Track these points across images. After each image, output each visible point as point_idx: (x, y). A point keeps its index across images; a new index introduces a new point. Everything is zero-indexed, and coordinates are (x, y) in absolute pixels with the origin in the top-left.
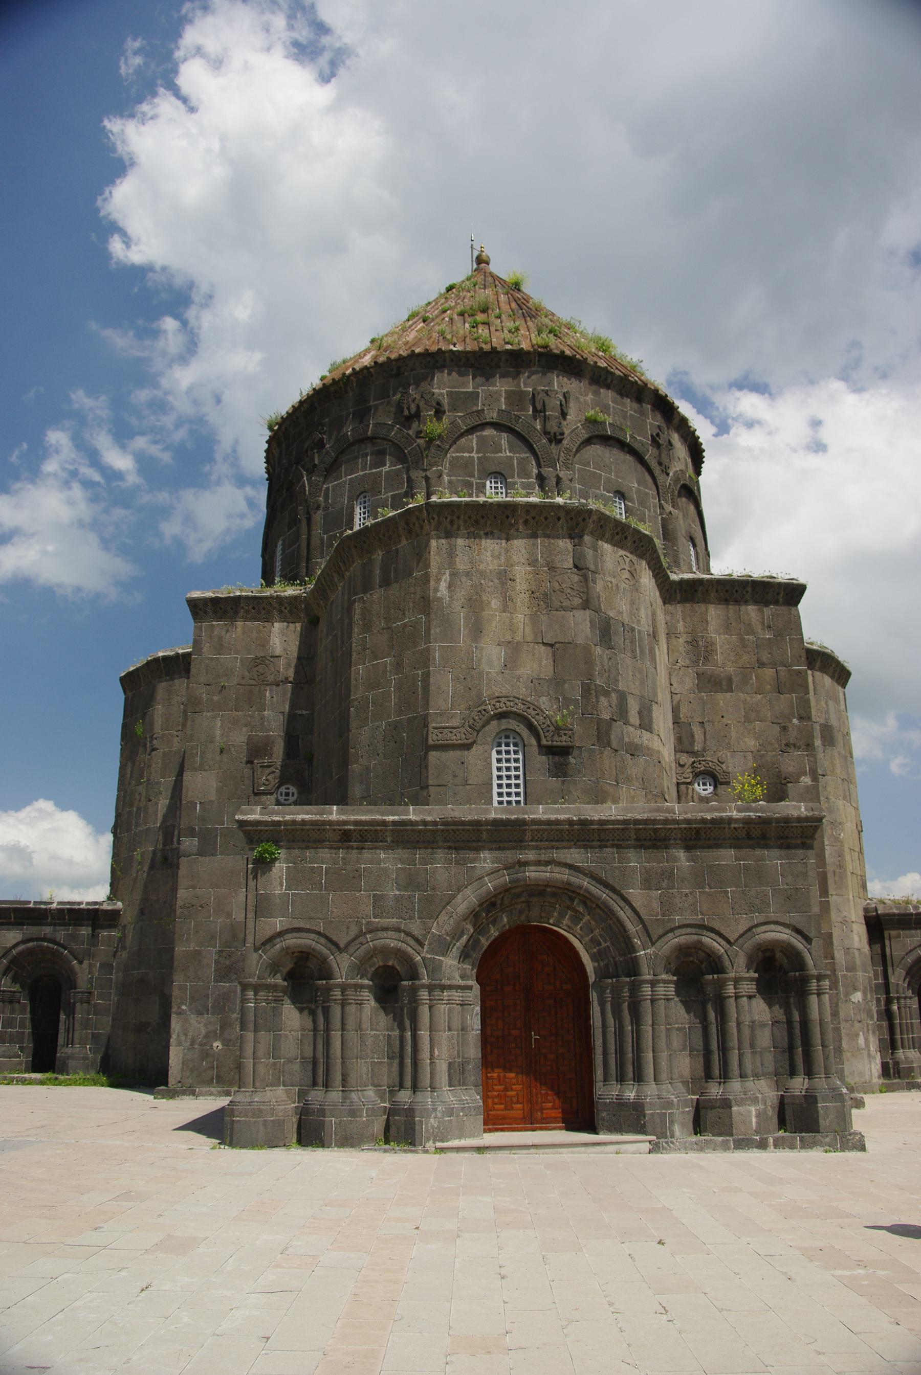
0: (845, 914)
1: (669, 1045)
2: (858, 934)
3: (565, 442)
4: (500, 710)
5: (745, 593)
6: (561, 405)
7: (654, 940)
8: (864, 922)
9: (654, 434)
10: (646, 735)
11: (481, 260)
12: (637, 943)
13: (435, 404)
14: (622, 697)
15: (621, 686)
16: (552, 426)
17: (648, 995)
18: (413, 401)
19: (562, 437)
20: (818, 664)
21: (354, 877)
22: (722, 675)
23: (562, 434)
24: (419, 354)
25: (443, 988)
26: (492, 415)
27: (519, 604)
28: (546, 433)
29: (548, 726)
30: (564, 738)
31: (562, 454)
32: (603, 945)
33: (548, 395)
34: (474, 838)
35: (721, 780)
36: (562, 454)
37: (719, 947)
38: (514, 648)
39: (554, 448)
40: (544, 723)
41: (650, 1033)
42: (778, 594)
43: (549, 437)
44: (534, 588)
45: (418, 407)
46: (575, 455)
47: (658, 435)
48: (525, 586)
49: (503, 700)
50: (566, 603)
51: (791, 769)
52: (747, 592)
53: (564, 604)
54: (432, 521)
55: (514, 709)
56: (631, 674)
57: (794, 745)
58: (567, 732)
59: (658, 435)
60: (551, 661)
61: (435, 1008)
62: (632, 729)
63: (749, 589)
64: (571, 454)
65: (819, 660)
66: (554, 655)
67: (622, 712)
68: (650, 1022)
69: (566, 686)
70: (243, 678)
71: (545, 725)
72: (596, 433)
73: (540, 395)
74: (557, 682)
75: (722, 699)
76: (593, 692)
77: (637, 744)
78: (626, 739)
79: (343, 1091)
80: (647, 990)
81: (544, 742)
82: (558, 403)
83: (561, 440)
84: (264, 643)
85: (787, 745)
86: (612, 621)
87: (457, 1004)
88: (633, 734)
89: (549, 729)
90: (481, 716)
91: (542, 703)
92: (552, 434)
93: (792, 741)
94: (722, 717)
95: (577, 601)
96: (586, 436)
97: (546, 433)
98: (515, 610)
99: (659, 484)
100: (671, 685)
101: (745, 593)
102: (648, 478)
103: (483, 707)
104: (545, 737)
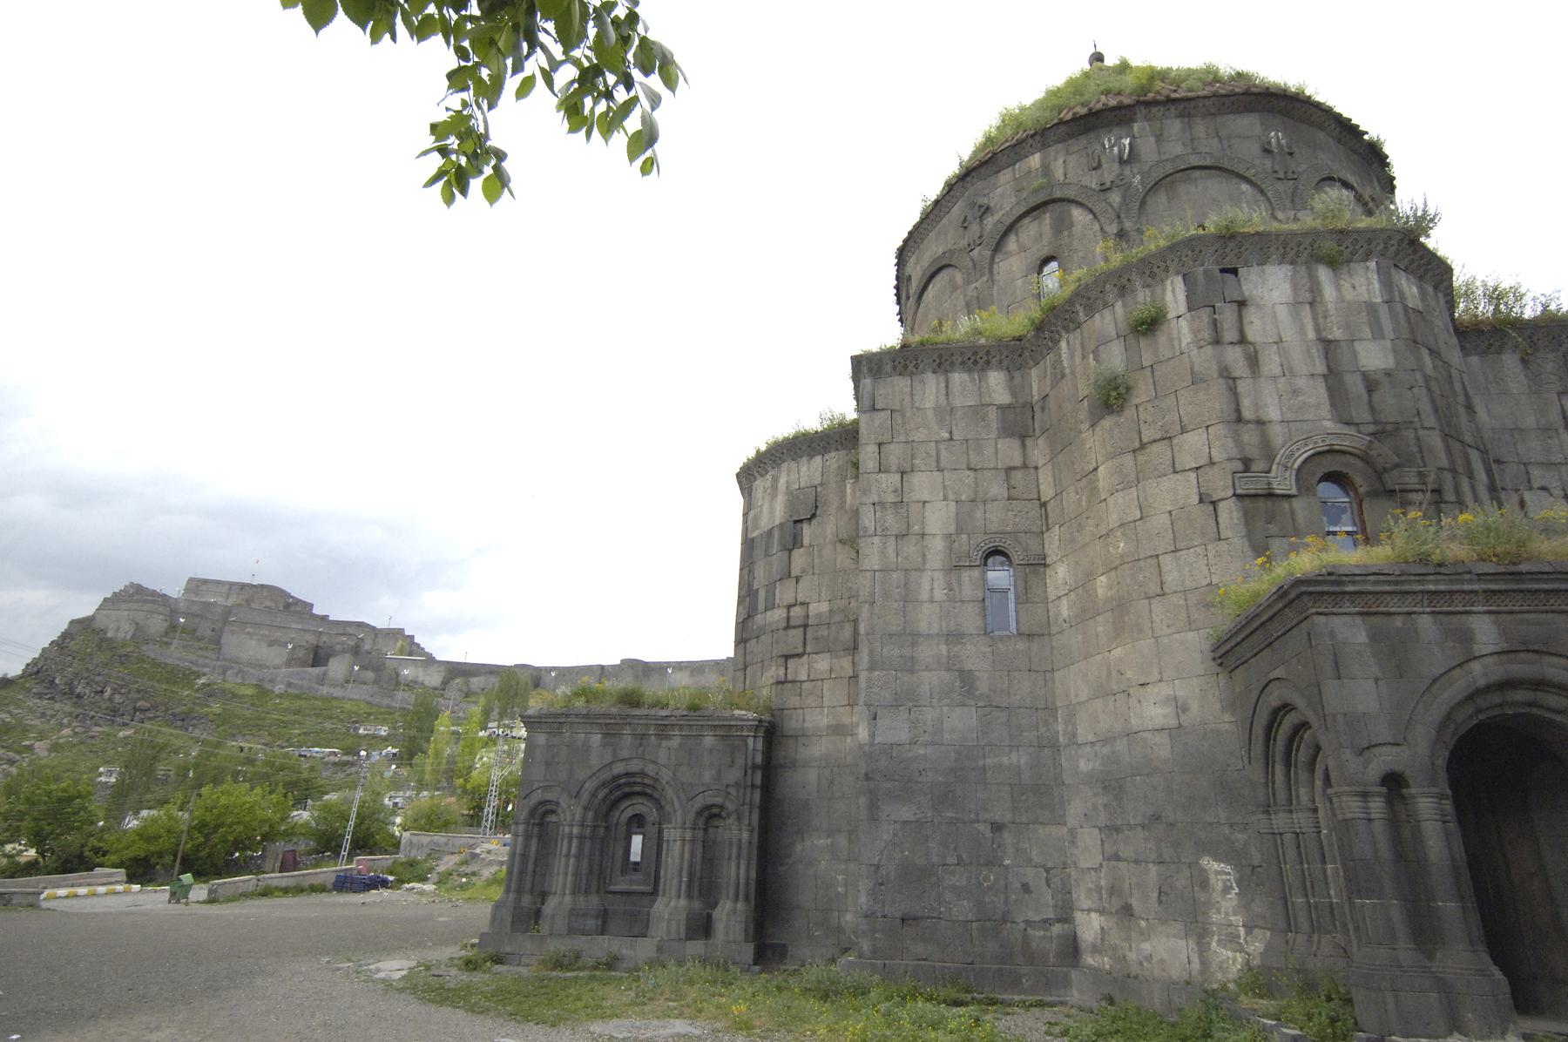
11: (1098, 58)
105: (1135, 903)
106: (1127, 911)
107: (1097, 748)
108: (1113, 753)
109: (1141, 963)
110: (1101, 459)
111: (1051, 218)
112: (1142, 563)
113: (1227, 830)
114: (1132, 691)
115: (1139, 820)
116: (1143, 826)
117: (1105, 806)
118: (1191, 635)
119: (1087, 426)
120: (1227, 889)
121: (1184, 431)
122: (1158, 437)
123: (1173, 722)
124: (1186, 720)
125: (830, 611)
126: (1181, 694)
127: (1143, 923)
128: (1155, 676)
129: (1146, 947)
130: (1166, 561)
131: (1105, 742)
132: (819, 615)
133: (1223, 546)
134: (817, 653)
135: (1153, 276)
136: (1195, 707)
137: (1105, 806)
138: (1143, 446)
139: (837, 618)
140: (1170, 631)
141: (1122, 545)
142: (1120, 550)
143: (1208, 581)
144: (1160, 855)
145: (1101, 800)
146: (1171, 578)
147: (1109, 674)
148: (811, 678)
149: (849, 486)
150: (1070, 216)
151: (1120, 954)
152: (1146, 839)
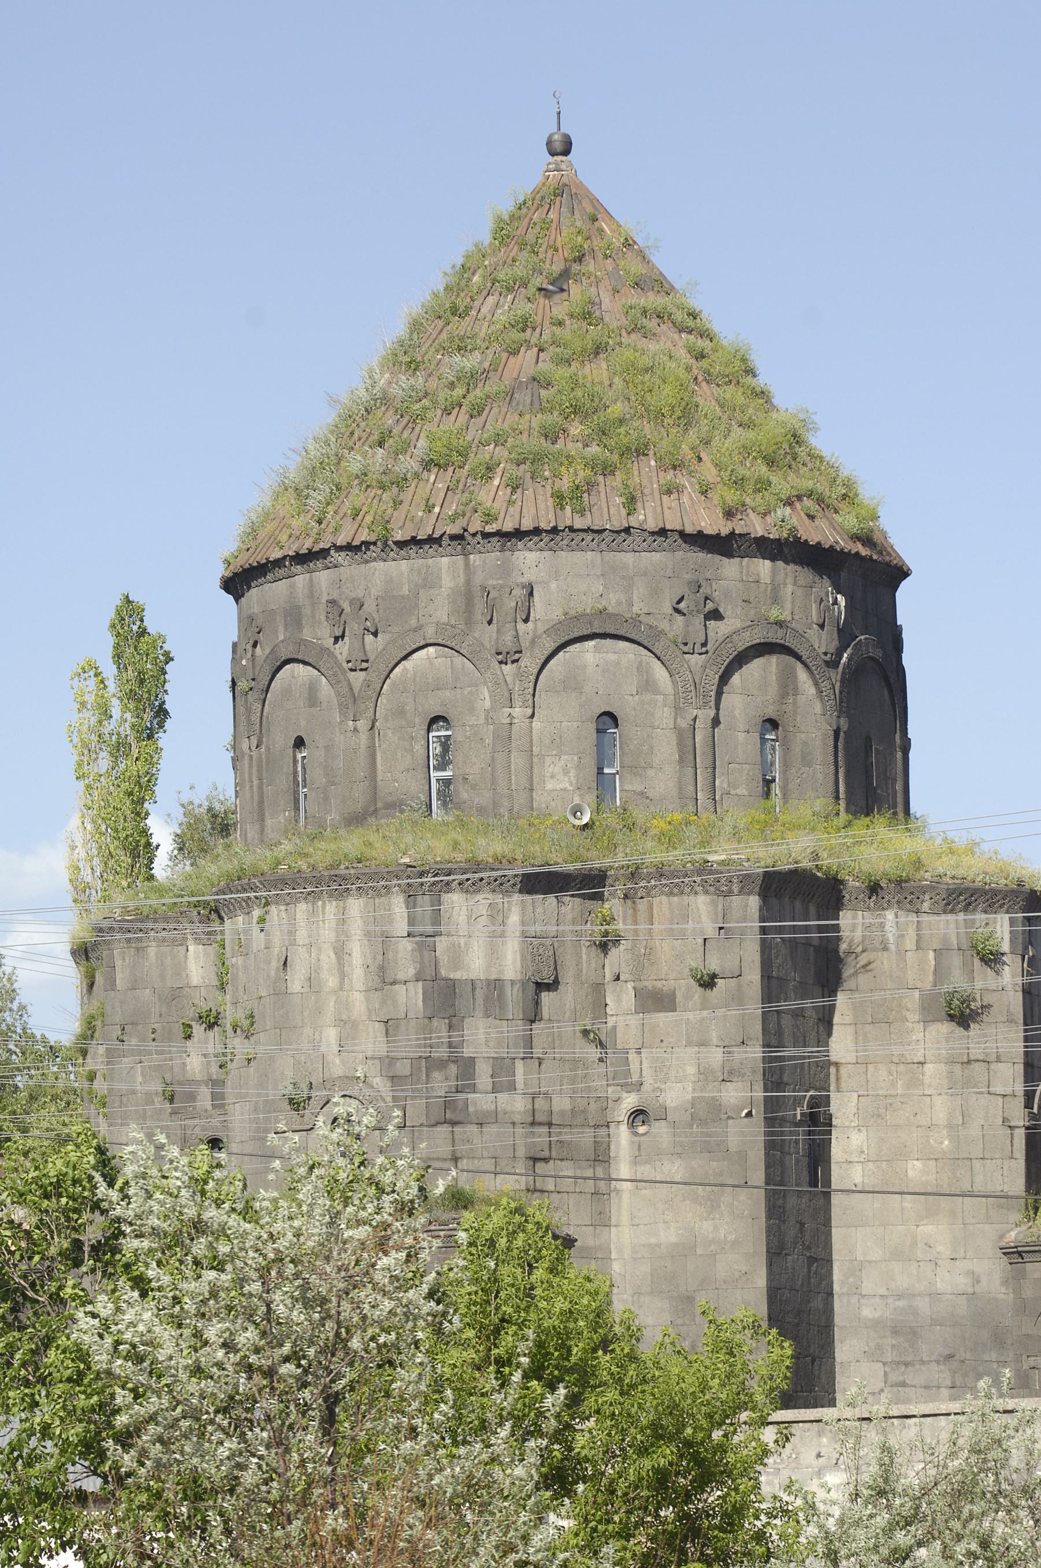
3: (522, 663)
10: (503, 1097)
14: (469, 1064)
15: (467, 1052)
27: (354, 980)
36: (518, 682)
38: (348, 1027)
44: (369, 962)
48: (360, 962)
50: (401, 976)
69: (398, 1064)
70: (161, 1015)
75: (662, 1019)
78: (471, 1109)
82: (513, 604)
84: (180, 969)
85: (730, 1073)
86: (457, 983)
95: (411, 972)
107: (890, 1300)
110: (929, 1057)
111: (778, 664)
112: (960, 1162)
113: (995, 1366)
114: (940, 1262)
115: (934, 1358)
116: (938, 1362)
117: (893, 1346)
118: (987, 1227)
119: (917, 1017)
121: (999, 1060)
122: (981, 1058)
123: (970, 1290)
124: (978, 1289)
126: (977, 1269)
128: (962, 1254)
130: (977, 1164)
131: (900, 1297)
132: (562, 1113)
133: (1013, 1163)
134: (562, 1160)
136: (984, 1280)
137: (893, 1346)
138: (969, 1062)
139: (579, 1120)
140: (973, 1221)
141: (946, 1142)
142: (944, 1146)
144: (953, 1382)
145: (889, 1341)
146: (979, 1179)
147: (915, 1243)
148: (558, 1189)
149: (584, 949)
150: (796, 677)
152: (941, 1371)
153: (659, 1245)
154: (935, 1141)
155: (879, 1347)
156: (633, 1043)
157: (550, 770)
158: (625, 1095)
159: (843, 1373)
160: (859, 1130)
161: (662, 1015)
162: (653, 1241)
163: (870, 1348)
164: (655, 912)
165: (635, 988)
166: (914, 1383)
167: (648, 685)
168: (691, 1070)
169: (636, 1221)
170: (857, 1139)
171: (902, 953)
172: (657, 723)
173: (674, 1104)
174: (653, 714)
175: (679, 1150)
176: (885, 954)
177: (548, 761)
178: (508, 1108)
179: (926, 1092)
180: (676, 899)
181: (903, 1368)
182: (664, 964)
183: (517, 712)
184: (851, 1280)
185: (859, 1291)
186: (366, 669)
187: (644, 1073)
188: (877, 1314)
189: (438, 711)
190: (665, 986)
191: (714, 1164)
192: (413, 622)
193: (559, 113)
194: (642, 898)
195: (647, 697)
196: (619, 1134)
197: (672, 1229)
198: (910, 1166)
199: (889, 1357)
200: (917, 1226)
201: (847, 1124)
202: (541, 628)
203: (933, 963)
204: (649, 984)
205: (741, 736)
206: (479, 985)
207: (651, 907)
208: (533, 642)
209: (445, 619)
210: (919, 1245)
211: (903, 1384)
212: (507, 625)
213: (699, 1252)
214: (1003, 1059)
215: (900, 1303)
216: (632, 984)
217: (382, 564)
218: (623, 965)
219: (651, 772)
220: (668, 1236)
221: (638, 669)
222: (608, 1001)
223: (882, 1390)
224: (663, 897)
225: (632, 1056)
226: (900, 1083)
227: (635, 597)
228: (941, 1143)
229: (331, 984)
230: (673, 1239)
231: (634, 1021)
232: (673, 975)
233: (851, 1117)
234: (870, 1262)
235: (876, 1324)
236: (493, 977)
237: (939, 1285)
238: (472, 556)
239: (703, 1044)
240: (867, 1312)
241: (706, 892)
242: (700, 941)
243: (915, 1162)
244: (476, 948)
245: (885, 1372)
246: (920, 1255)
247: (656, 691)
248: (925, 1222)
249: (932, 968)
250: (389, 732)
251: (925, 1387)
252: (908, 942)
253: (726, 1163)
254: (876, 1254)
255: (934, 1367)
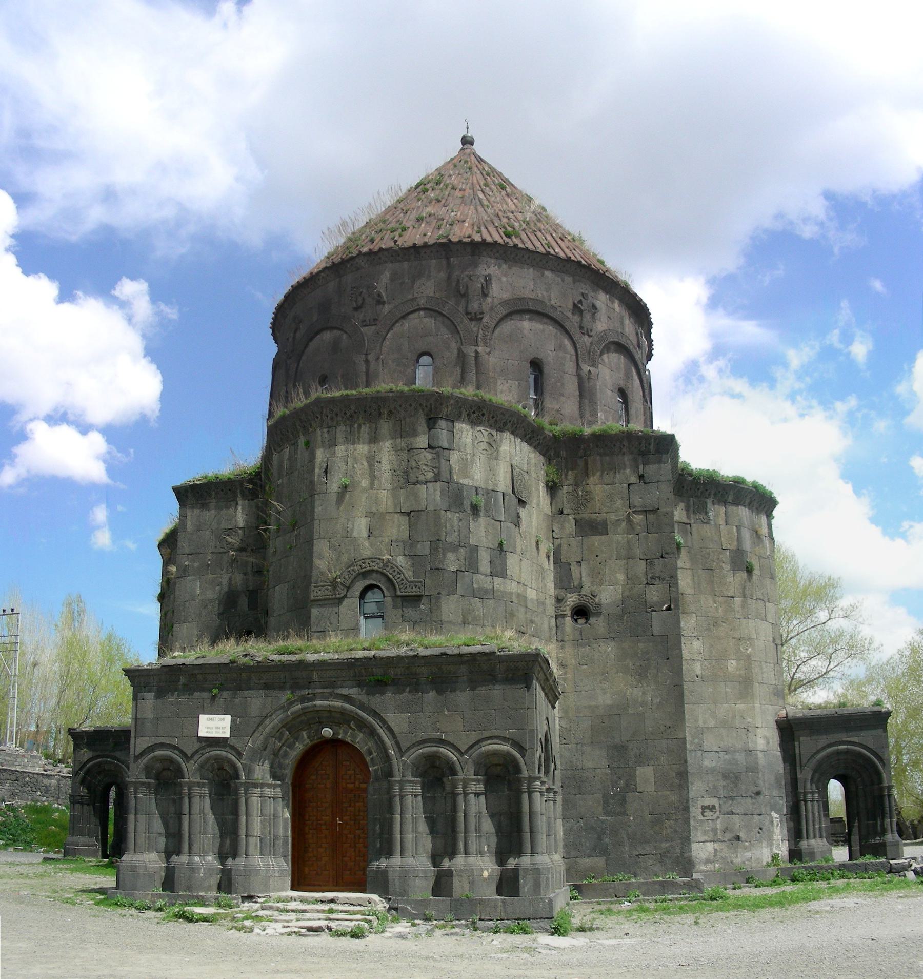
0: (749, 720)
1: (415, 830)
2: (765, 737)
3: (484, 320)
4: (365, 569)
5: (622, 447)
6: (483, 287)
7: (403, 750)
8: (776, 727)
9: (576, 302)
10: (498, 581)
12: (391, 753)
13: (376, 297)
15: (473, 541)
16: (474, 306)
17: (397, 792)
18: (360, 295)
19: (481, 316)
20: (730, 498)
21: (198, 707)
22: (599, 519)
23: (482, 313)
24: (365, 254)
25: (256, 786)
26: (422, 302)
28: (467, 313)
29: (402, 580)
30: (415, 589)
31: (481, 331)
32: (375, 754)
33: (471, 279)
34: (339, 671)
35: (593, 611)
36: (481, 331)
37: (454, 757)
39: (473, 326)
40: (399, 578)
41: (399, 820)
42: (650, 444)
43: (470, 317)
45: (364, 299)
46: (493, 331)
47: (580, 302)
49: (367, 561)
51: (655, 599)
52: (624, 446)
53: (420, 479)
54: (316, 419)
55: (376, 568)
56: (483, 530)
57: (659, 578)
58: (417, 584)
59: (580, 302)
60: (408, 526)
61: (249, 800)
62: (483, 577)
63: (625, 443)
64: (490, 330)
65: (732, 493)
66: (410, 522)
67: (472, 565)
68: (399, 811)
69: (419, 546)
71: (400, 579)
72: (515, 308)
73: (465, 280)
74: (412, 542)
75: (596, 540)
76: (440, 549)
77: (487, 589)
78: (475, 586)
79: (189, 856)
80: (397, 789)
81: (399, 593)
82: (480, 286)
83: (482, 318)
85: (653, 578)
87: (257, 797)
88: (482, 581)
89: (403, 582)
90: (350, 575)
91: (398, 561)
92: (473, 314)
93: (657, 575)
94: (597, 556)
96: (504, 312)
97: (467, 313)
98: (380, 487)
99: (578, 347)
100: (553, 531)
101: (622, 447)
102: (567, 343)
103: (352, 568)
104: (400, 589)
105: (742, 835)
106: (738, 838)
108: (734, 759)
109: (744, 863)
114: (750, 729)
115: (750, 794)
116: (751, 797)
118: (770, 707)
119: (729, 567)
120: (778, 824)
125: (537, 600)
126: (768, 735)
127: (747, 844)
129: (748, 855)
135: (760, 506)
137: (724, 786)
141: (750, 649)
143: (774, 683)
149: (541, 487)
151: (729, 861)
153: (597, 707)
154: (743, 648)
155: (715, 787)
156: (574, 559)
157: (500, 388)
158: (569, 595)
159: (693, 805)
160: (698, 639)
161: (597, 538)
162: (593, 703)
163: (710, 788)
164: (589, 467)
165: (575, 519)
166: (738, 811)
167: (560, 347)
168: (621, 577)
169: (578, 689)
170: (697, 645)
171: (718, 527)
172: (566, 370)
173: (609, 601)
174: (564, 365)
175: (612, 635)
176: (708, 525)
177: (499, 382)
178: (502, 589)
179: (736, 616)
180: (607, 458)
181: (731, 802)
182: (597, 502)
183: (480, 349)
184: (696, 740)
185: (702, 748)
186: (376, 324)
187: (583, 579)
188: (714, 764)
189: (423, 348)
190: (600, 517)
191: (641, 645)
192: (410, 297)
193: (467, 128)
194: (581, 457)
195: (561, 354)
196: (564, 624)
197: (608, 695)
198: (729, 664)
199: (722, 793)
200: (736, 704)
201: (690, 634)
202: (496, 302)
203: (736, 534)
204: (585, 515)
205: (609, 392)
206: (480, 492)
207: (586, 463)
208: (492, 309)
209: (432, 295)
210: (737, 717)
211: (733, 813)
212: (476, 297)
213: (631, 711)
214: (771, 601)
215: (727, 757)
216: (573, 516)
217: (391, 265)
218: (565, 503)
219: (563, 399)
220: (605, 699)
221: (555, 336)
222: (554, 529)
223: (718, 818)
224: (598, 458)
225: (574, 568)
226: (721, 609)
227: (552, 295)
228: (747, 650)
229: (363, 485)
230: (609, 702)
231: (574, 542)
232: (605, 510)
233: (693, 630)
234: (708, 728)
235: (712, 771)
236: (491, 488)
237: (750, 745)
238: (452, 259)
239: (629, 558)
240: (707, 763)
241: (632, 453)
242: (625, 485)
243: (732, 662)
244: (479, 465)
245: (720, 804)
246: (738, 725)
247: (565, 351)
248: (739, 702)
249: (736, 537)
250: (390, 363)
251: (744, 814)
252: (720, 519)
253: (651, 644)
254: (712, 723)
255: (749, 800)
